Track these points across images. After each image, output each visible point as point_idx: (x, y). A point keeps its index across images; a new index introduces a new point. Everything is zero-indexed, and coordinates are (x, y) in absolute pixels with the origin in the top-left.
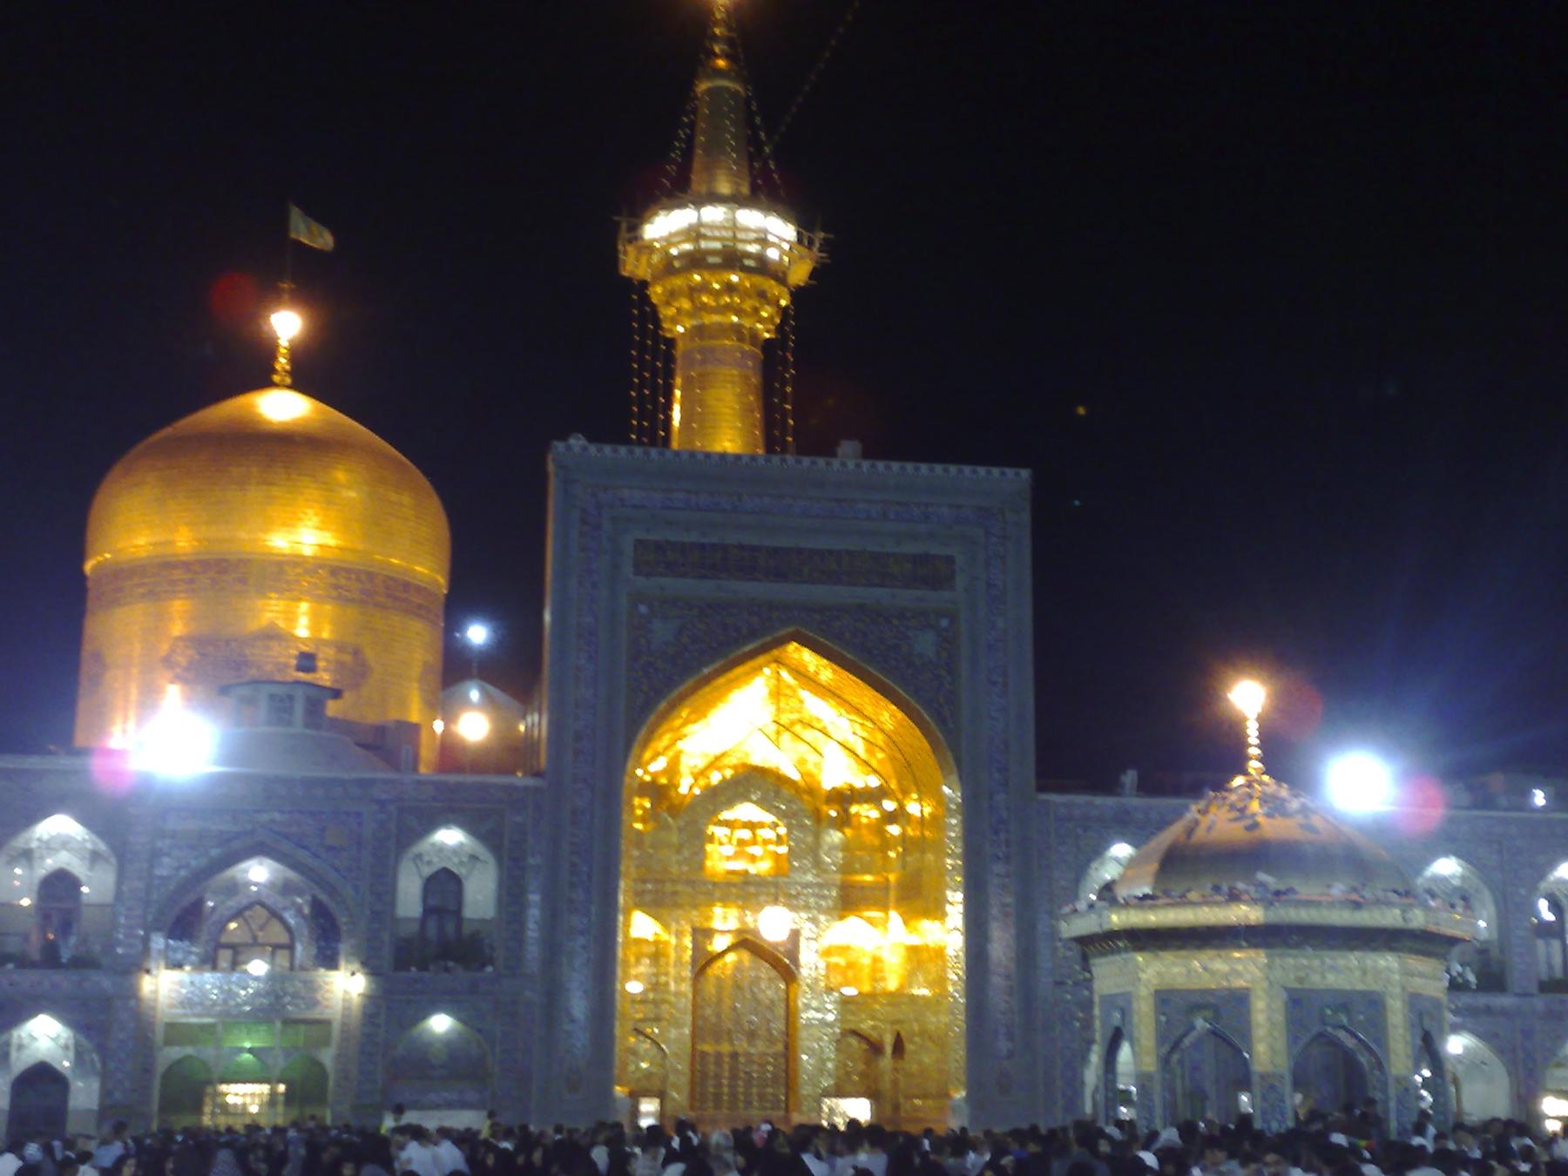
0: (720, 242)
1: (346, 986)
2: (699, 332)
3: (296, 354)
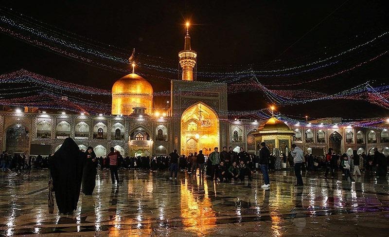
2: (185, 67)
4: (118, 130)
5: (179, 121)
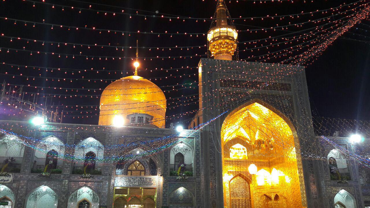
0: (222, 37)
1: (157, 180)
3: (138, 70)
4: (91, 155)
5: (217, 134)
